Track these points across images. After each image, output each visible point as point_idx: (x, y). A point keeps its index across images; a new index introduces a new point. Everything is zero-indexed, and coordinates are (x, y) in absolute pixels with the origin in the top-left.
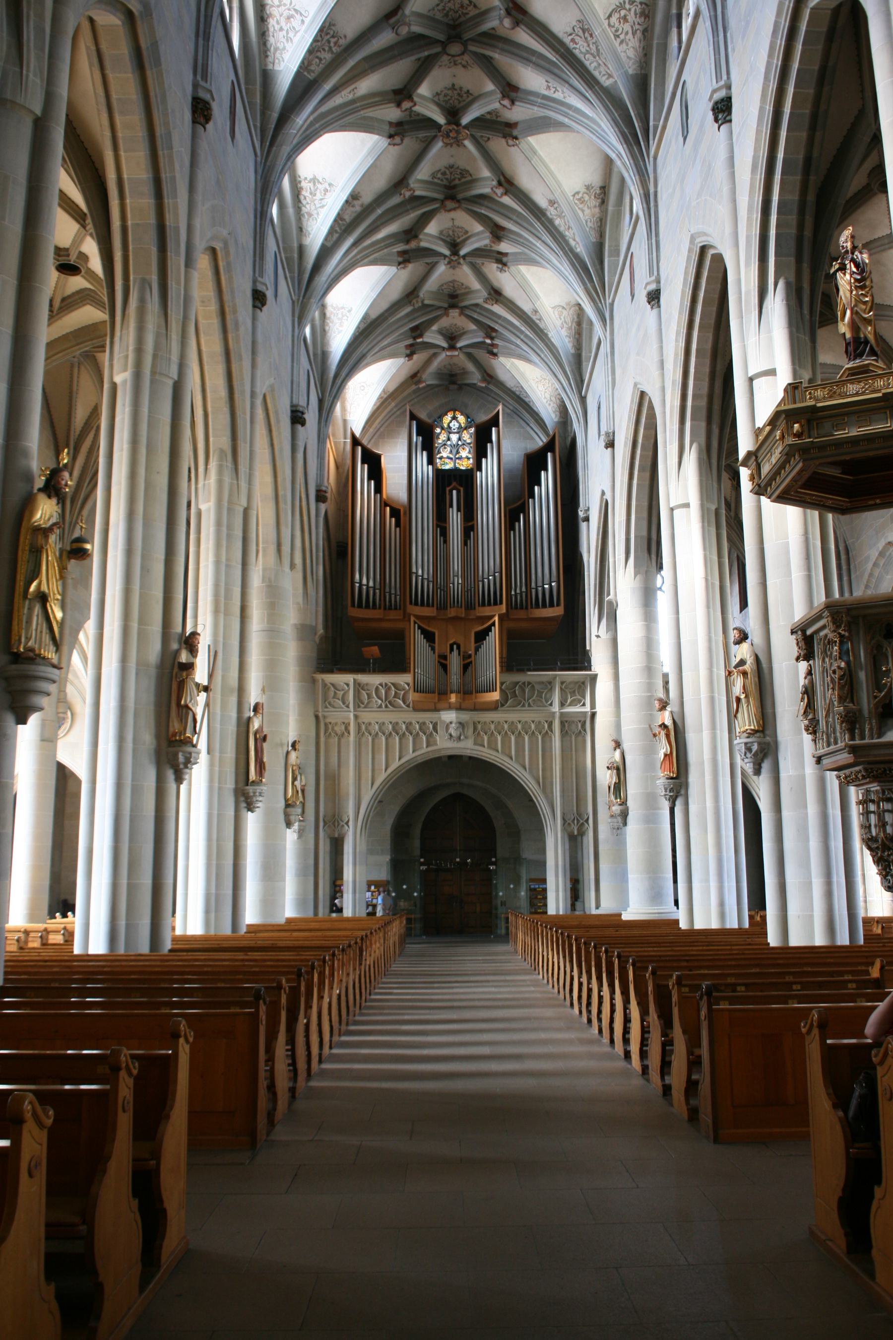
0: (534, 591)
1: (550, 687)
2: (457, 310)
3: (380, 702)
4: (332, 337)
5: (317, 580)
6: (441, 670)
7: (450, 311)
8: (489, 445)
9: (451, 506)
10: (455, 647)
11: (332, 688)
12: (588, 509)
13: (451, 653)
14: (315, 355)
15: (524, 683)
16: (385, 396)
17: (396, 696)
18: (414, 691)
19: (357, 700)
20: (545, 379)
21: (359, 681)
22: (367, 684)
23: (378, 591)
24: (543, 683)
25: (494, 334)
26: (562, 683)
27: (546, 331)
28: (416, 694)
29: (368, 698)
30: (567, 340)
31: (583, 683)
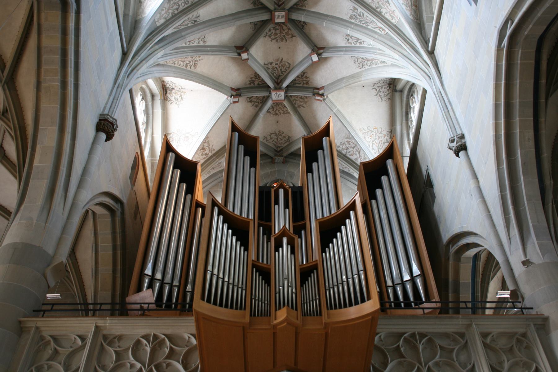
0: (390, 290)
1: (463, 342)
2: (283, 13)
3: (139, 365)
4: (147, 5)
5: (73, 205)
6: (258, 279)
7: (276, 14)
8: (320, 152)
9: (277, 202)
10: (285, 240)
11: (52, 343)
12: (462, 137)
13: (277, 250)
14: (125, 15)
15: (413, 335)
16: (210, 154)
17: (172, 354)
18: (203, 299)
19: (95, 363)
20: (372, 131)
21: (105, 332)
22: (120, 338)
23: (176, 290)
24: (446, 335)
25: (321, 51)
26: (484, 335)
27: (378, 10)
28: (205, 304)
29: (118, 360)
30: (404, 7)
31: (524, 335)
